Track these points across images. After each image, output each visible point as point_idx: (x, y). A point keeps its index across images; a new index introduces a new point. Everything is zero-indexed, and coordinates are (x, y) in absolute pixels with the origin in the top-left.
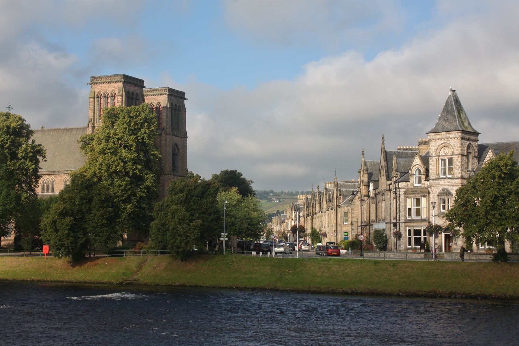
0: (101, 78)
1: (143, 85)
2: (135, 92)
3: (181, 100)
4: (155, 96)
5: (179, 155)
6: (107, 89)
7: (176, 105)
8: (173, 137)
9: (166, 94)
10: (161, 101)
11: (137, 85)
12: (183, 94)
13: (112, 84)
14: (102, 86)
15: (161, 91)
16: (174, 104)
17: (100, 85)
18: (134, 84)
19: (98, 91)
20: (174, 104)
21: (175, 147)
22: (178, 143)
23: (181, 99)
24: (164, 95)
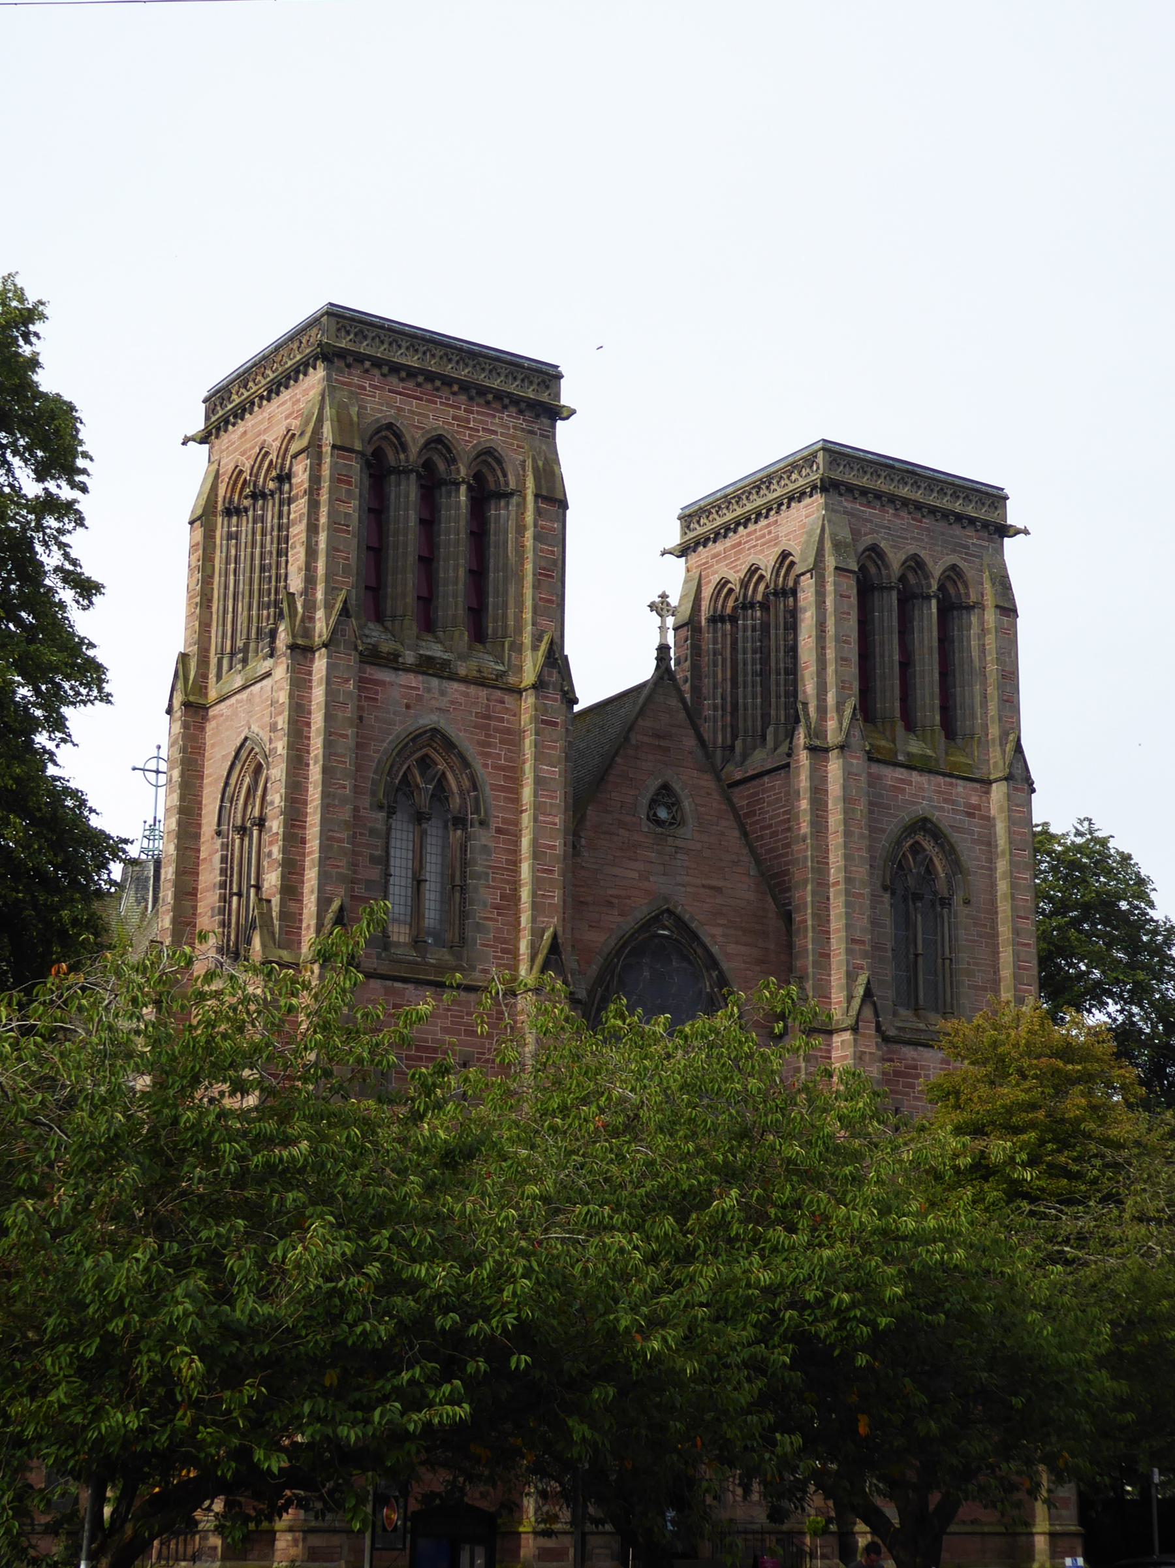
0: (243, 377)
1: (557, 396)
2: (467, 442)
3: (971, 537)
4: (763, 522)
5: (967, 902)
6: (263, 437)
7: (916, 564)
8: (892, 775)
9: (814, 488)
10: (795, 548)
11: (482, 391)
12: (995, 498)
13: (285, 395)
14: (245, 432)
15: (794, 477)
16: (896, 559)
17: (241, 426)
18: (448, 381)
19: (231, 466)
20: (896, 559)
21: (928, 845)
22: (944, 817)
23: (970, 532)
24: (807, 501)
